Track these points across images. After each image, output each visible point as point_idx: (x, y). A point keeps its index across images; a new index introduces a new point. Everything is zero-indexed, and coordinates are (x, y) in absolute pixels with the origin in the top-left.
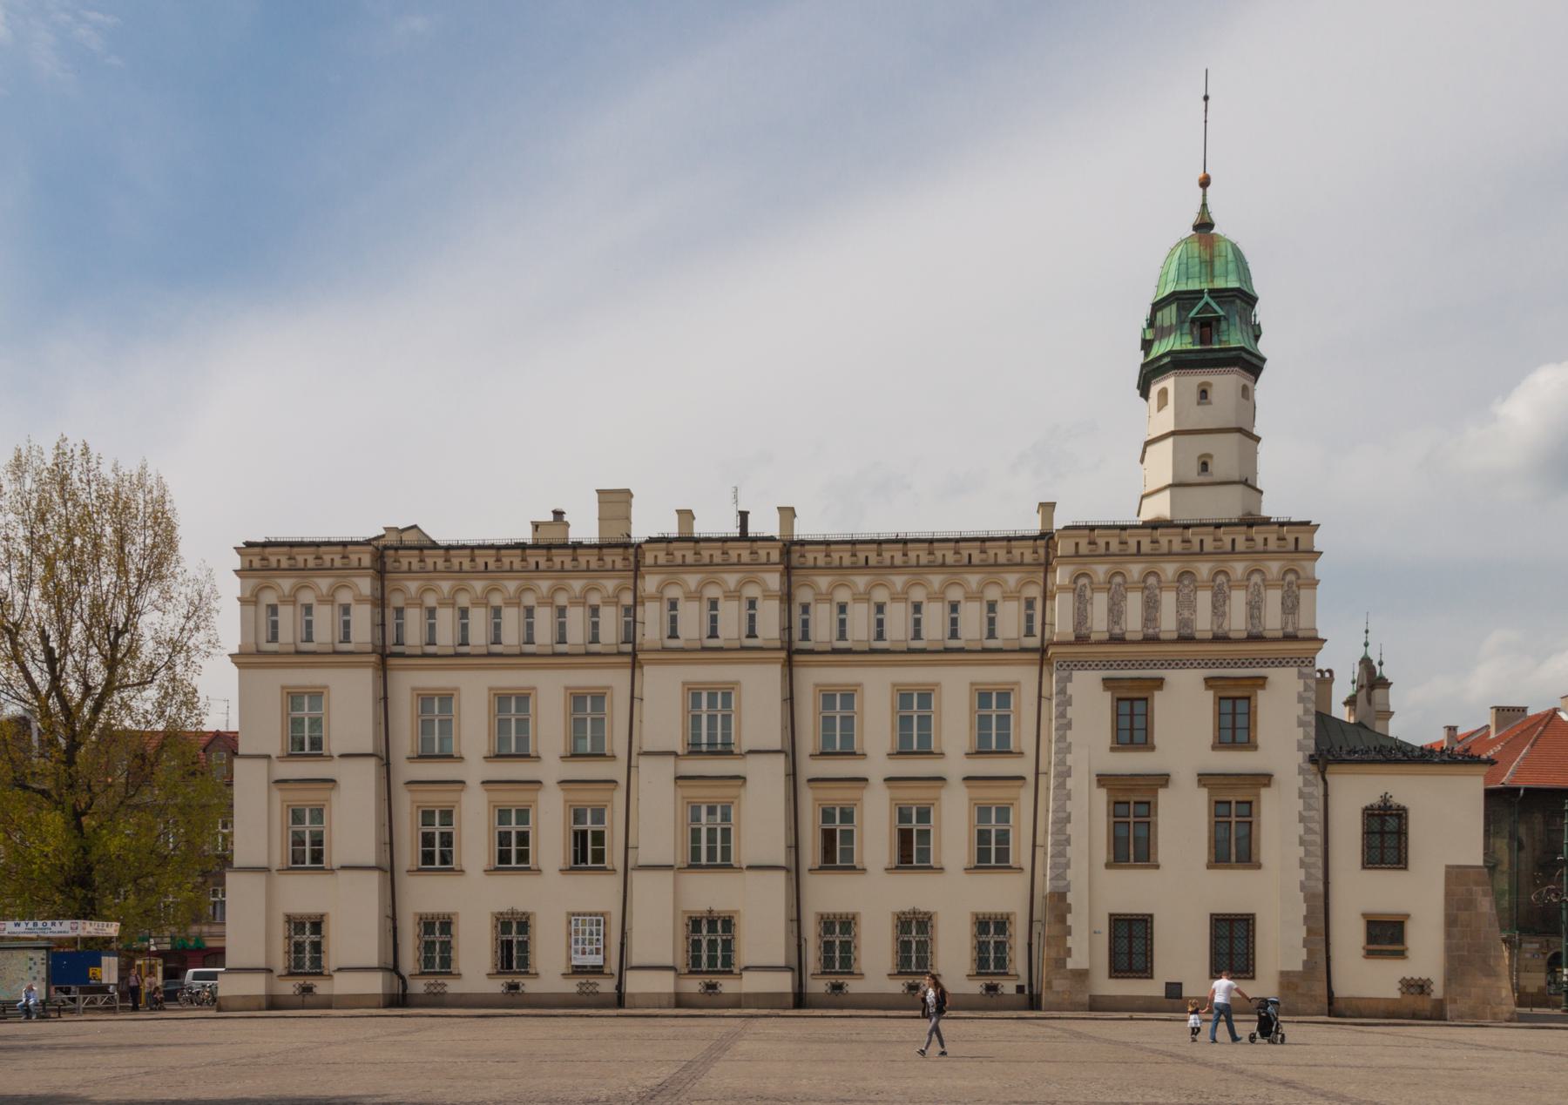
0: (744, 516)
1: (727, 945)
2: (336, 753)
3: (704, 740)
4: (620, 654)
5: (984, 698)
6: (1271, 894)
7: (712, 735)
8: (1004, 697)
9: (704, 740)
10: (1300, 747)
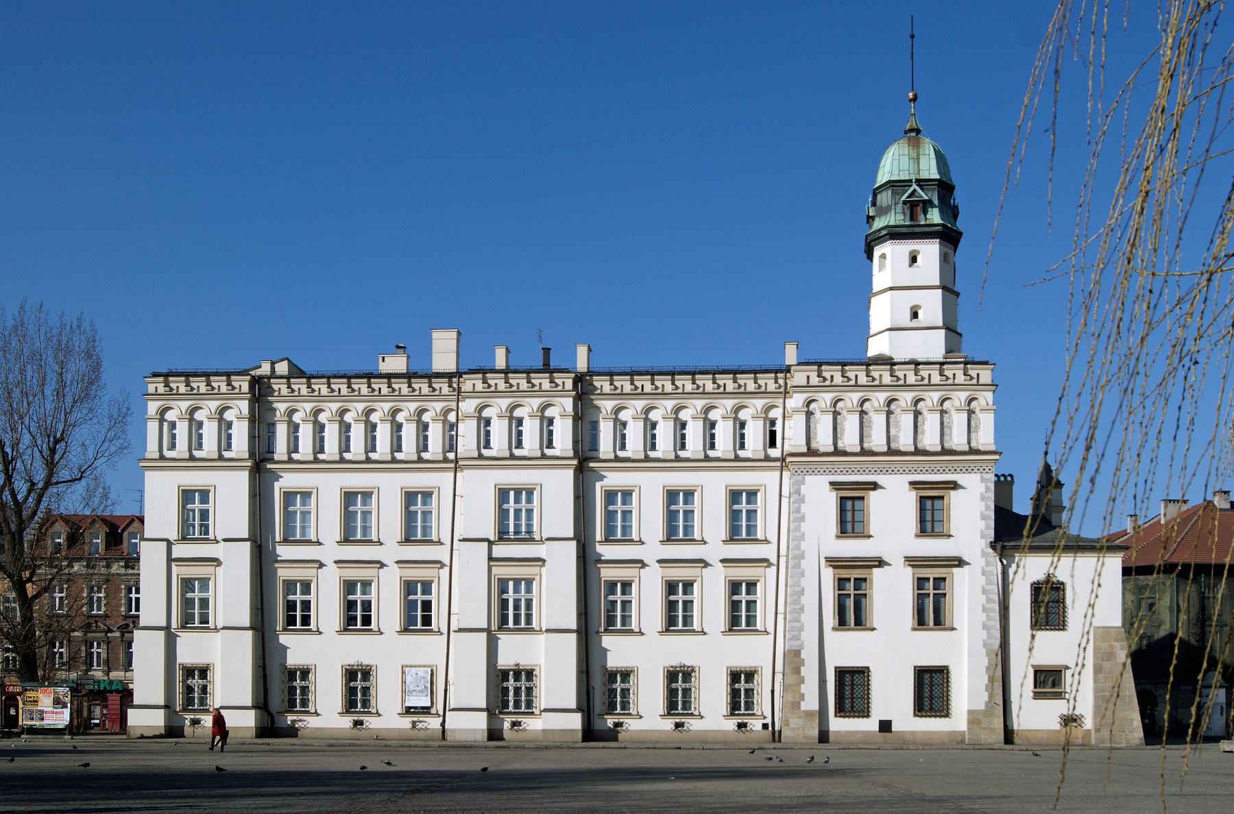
0: (547, 351)
1: (529, 690)
3: (511, 529)
5: (734, 496)
7: (517, 526)
8: (752, 495)
9: (511, 529)
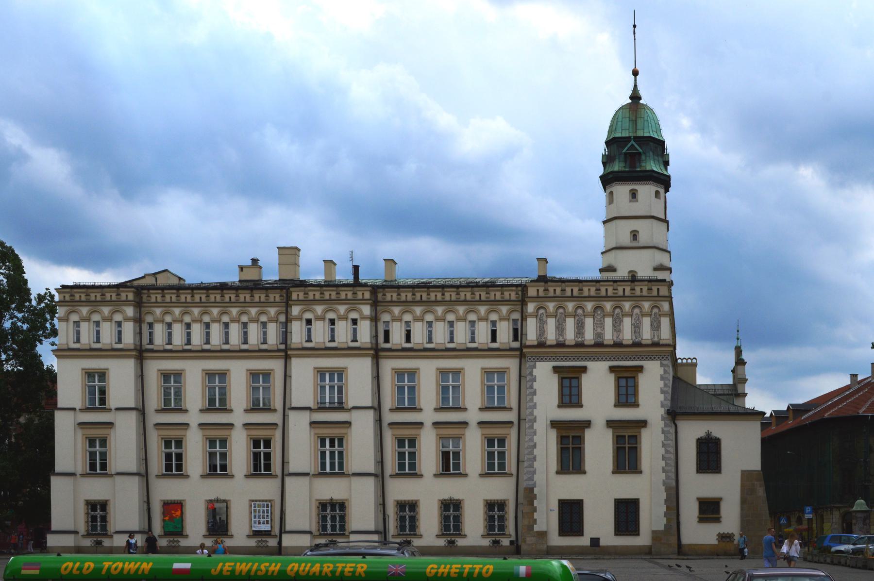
3: (327, 401)
4: (279, 350)
6: (645, 487)
9: (327, 401)
10: (662, 406)
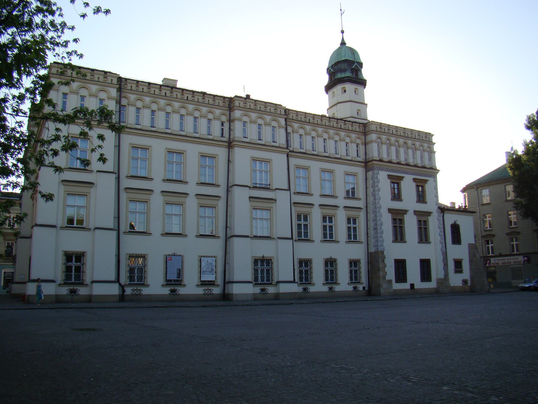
2: (95, 170)
